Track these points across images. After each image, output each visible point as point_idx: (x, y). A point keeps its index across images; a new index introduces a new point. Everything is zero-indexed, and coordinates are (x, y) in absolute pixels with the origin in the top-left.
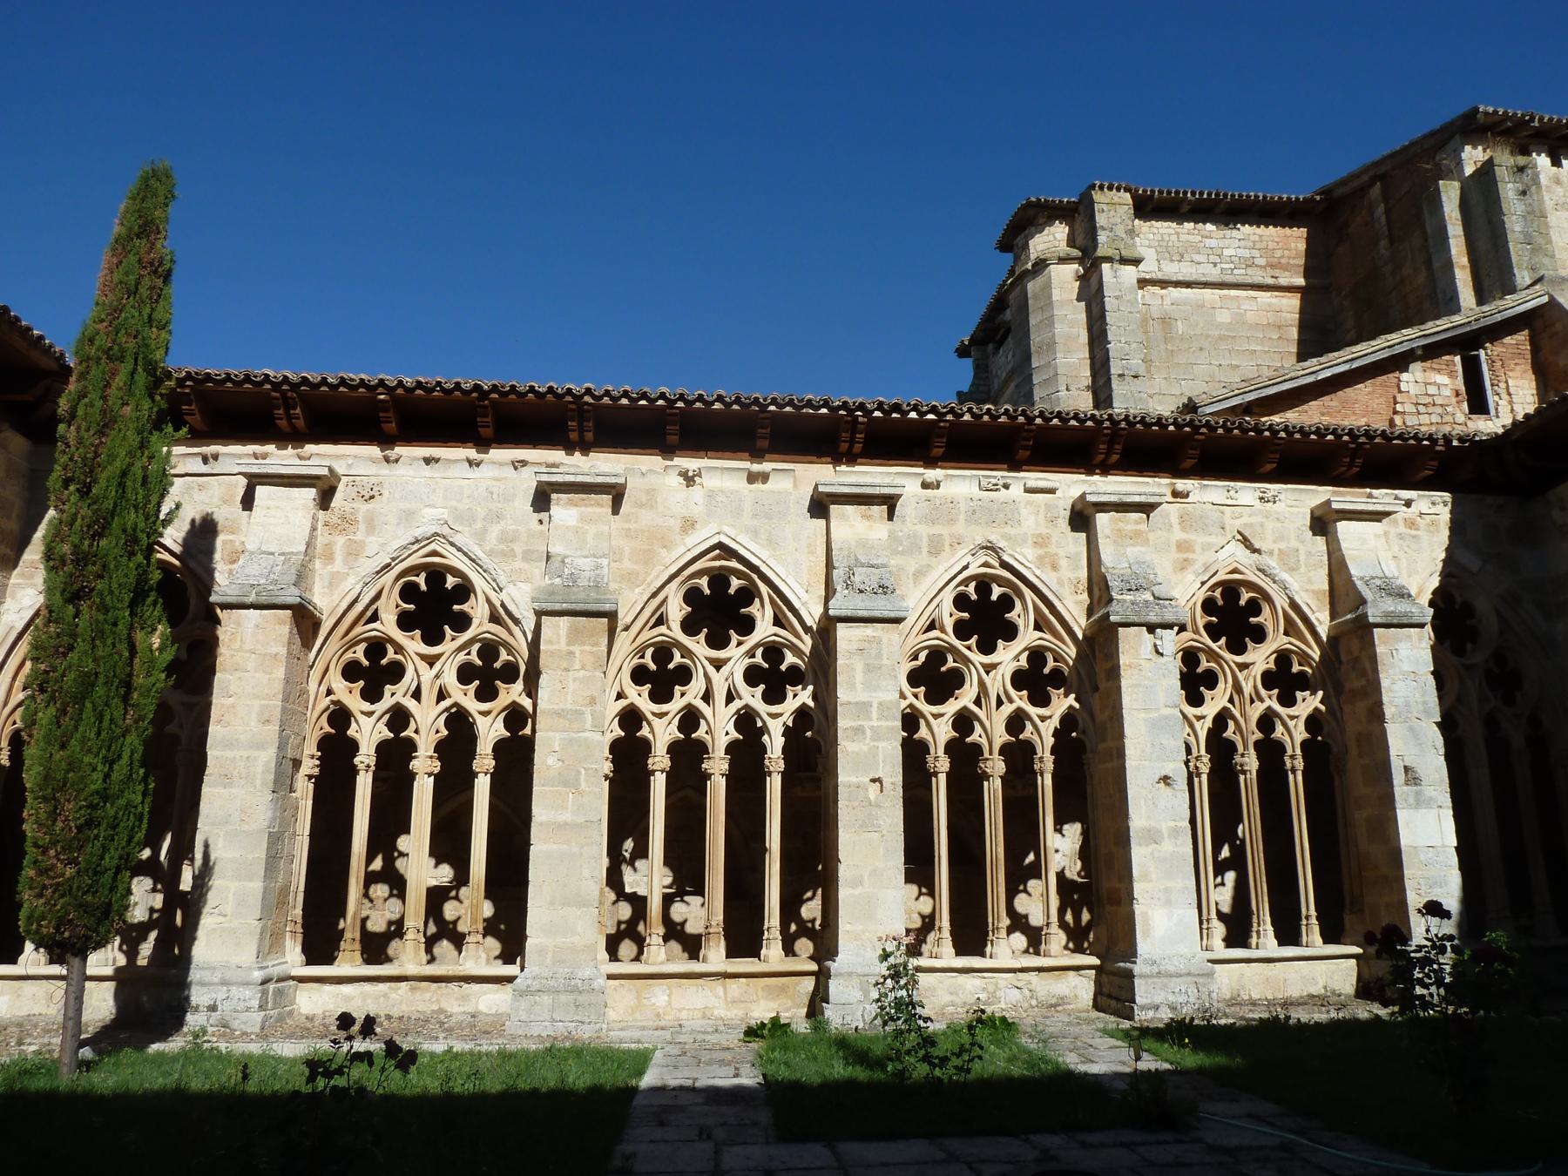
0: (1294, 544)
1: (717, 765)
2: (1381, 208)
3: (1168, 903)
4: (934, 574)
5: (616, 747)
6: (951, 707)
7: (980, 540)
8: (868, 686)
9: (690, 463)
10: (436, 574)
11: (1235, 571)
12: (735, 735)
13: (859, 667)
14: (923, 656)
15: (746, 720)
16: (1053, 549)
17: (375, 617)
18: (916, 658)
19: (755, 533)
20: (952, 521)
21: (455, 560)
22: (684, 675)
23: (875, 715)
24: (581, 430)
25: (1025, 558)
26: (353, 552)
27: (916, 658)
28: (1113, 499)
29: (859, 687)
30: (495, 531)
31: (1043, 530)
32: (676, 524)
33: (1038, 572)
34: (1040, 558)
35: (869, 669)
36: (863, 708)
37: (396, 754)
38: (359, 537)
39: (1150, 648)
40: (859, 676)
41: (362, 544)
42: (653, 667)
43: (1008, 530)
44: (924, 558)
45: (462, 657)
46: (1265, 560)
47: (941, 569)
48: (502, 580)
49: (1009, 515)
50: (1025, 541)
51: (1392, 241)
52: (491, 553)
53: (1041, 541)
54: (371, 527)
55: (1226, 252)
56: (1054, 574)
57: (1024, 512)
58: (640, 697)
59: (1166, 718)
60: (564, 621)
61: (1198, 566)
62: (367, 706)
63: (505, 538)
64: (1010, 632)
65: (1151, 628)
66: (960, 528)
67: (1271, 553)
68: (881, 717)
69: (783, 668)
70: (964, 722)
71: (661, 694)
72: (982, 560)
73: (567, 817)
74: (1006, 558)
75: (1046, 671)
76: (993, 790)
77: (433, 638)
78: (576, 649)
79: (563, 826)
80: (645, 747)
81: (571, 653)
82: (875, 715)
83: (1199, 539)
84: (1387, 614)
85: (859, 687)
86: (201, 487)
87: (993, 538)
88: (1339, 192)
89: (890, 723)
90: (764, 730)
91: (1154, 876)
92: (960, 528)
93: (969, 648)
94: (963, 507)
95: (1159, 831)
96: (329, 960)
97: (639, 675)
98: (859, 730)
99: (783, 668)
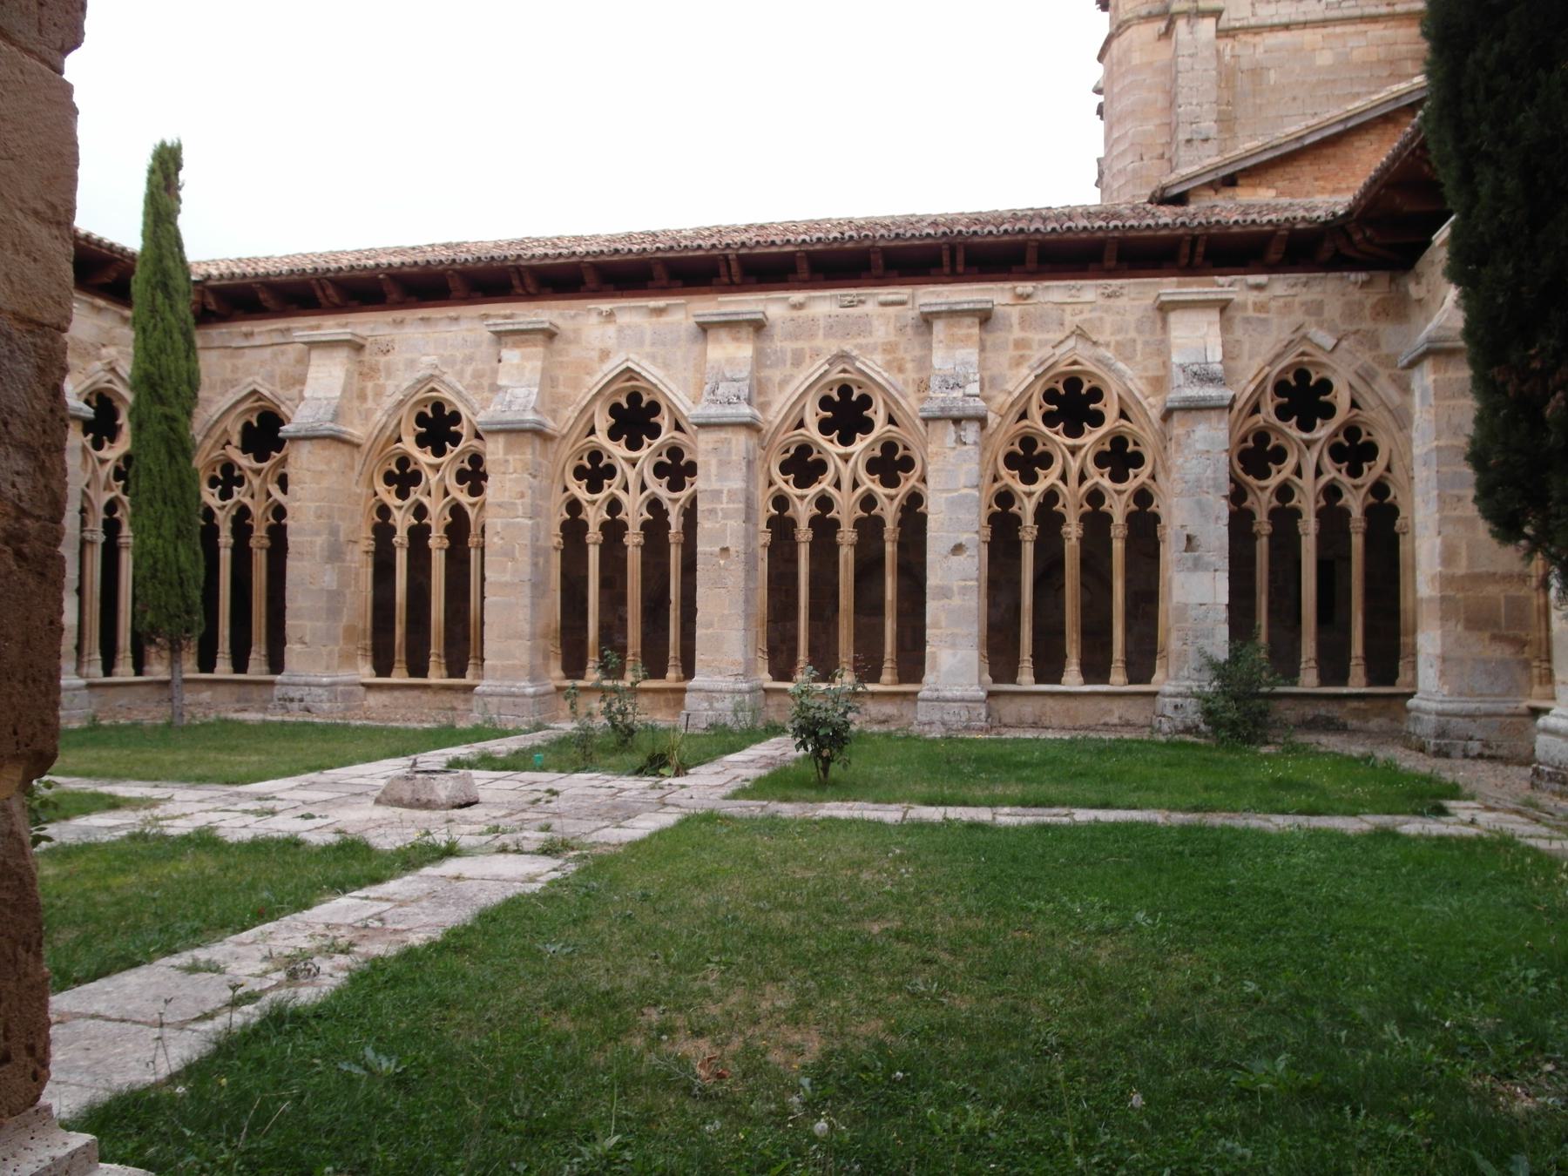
0: (1132, 334)
1: (633, 539)
3: (953, 646)
4: (796, 383)
5: (565, 526)
7: (834, 351)
8: (721, 477)
9: (605, 305)
10: (438, 406)
11: (1075, 363)
12: (647, 516)
13: (714, 462)
14: (792, 451)
15: (655, 505)
16: (901, 354)
17: (399, 440)
18: (787, 451)
19: (653, 358)
20: (812, 336)
21: (445, 394)
22: (610, 471)
23: (725, 499)
24: (523, 285)
25: (874, 366)
26: (379, 394)
27: (787, 451)
28: (944, 308)
29: (713, 478)
30: (469, 370)
31: (893, 338)
32: (595, 355)
35: (721, 464)
36: (716, 494)
37: (419, 534)
38: (382, 381)
39: (954, 436)
40: (714, 470)
41: (383, 387)
42: (588, 466)
43: (861, 340)
44: (788, 369)
45: (458, 466)
46: (1102, 351)
47: (802, 377)
48: (477, 406)
50: (875, 349)
52: (467, 387)
53: (889, 348)
54: (389, 375)
56: (901, 377)
57: (876, 323)
58: (579, 491)
59: (966, 496)
60: (501, 439)
61: (1034, 361)
62: (399, 502)
63: (478, 375)
64: (867, 426)
65: (957, 421)
66: (819, 342)
67: (1107, 345)
68: (730, 501)
69: (682, 463)
70: (824, 502)
71: (594, 487)
73: (507, 578)
74: (858, 364)
76: (846, 555)
77: (439, 451)
78: (510, 458)
79: (506, 584)
80: (584, 526)
81: (507, 461)
82: (725, 499)
83: (1035, 336)
84: (1187, 399)
85: (713, 478)
86: (283, 353)
87: (847, 348)
90: (666, 513)
92: (819, 342)
94: (822, 323)
95: (950, 589)
96: (388, 675)
97: (579, 473)
98: (712, 511)
99: (682, 463)
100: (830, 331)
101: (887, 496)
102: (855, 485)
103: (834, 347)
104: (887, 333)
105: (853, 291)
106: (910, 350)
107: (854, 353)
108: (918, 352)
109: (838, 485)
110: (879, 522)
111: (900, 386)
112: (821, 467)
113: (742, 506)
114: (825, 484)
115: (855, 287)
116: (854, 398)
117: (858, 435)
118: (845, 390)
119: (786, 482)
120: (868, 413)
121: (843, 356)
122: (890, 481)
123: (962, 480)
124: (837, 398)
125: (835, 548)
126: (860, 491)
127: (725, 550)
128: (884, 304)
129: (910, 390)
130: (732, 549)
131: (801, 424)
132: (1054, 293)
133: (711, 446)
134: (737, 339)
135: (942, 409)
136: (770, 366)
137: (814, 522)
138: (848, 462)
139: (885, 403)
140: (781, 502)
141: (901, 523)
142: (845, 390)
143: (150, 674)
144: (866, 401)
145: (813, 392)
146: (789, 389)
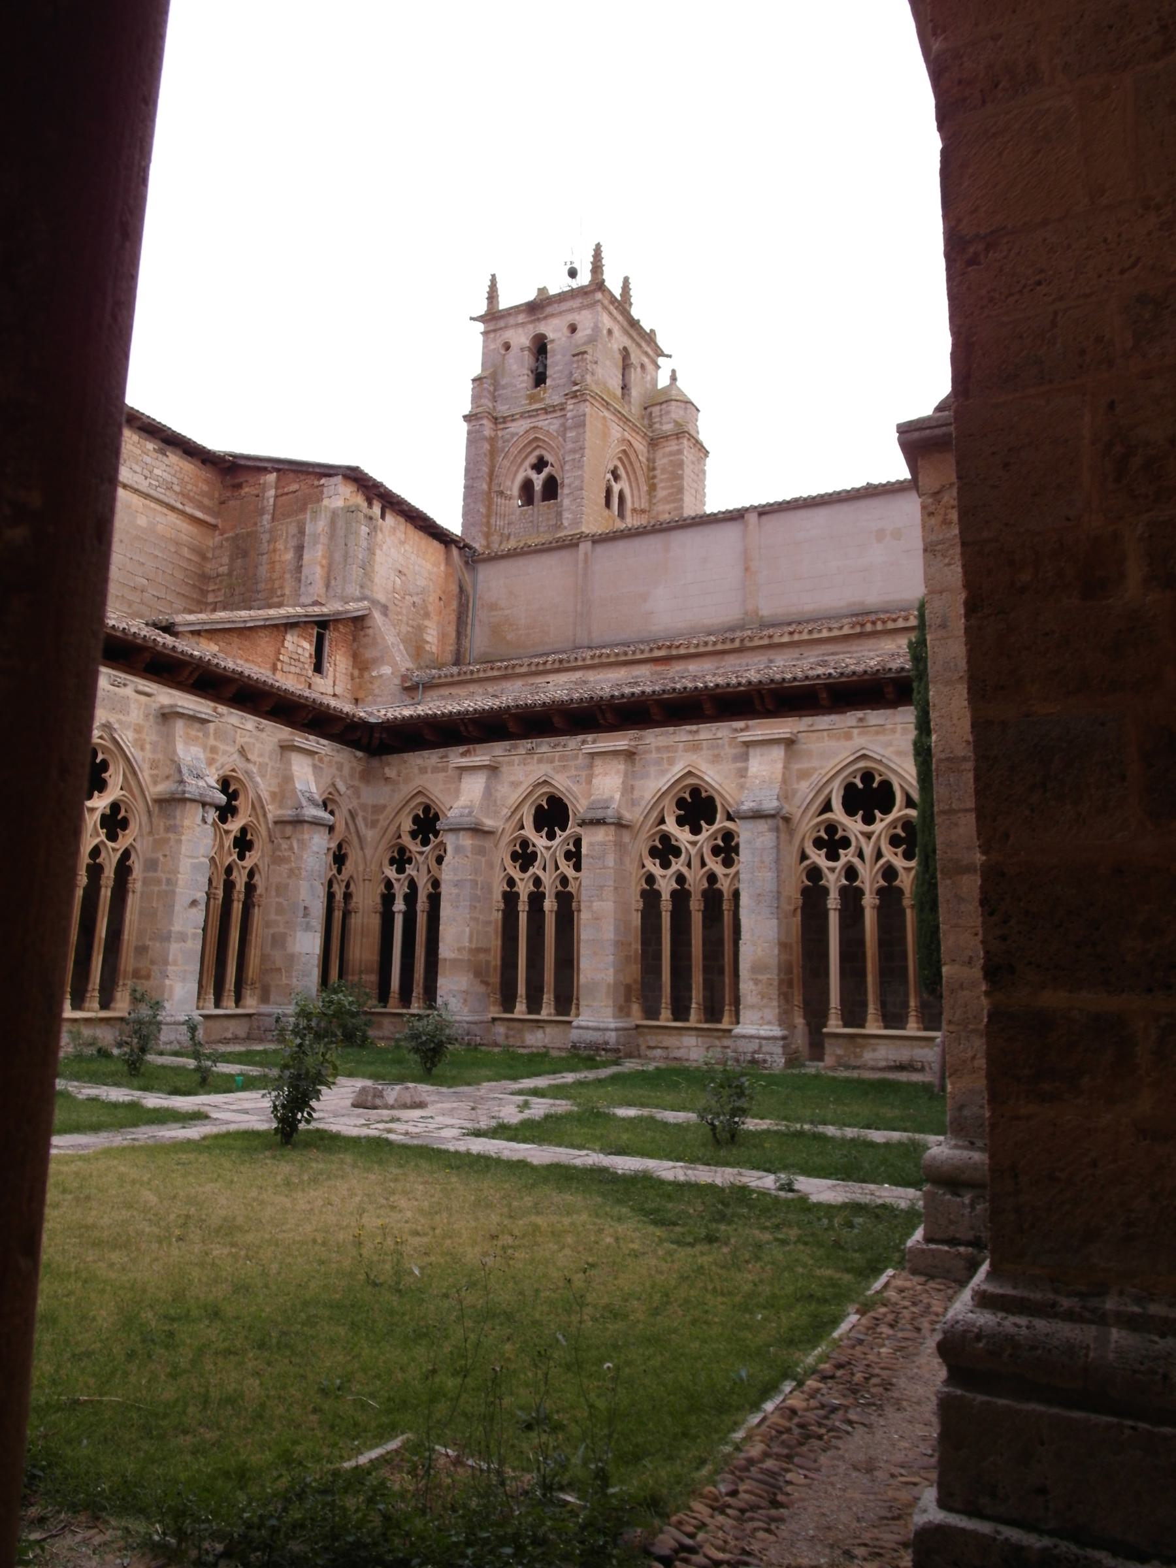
0: (267, 760)
2: (272, 492)
3: (184, 980)
11: (233, 770)
16: (144, 736)
31: (141, 722)
34: (136, 740)
46: (251, 767)
51: (273, 519)
53: (138, 729)
55: (157, 472)
57: (132, 706)
59: (202, 863)
61: (218, 764)
65: (204, 804)
67: (255, 763)
75: (119, 817)
83: (222, 747)
84: (314, 817)
87: (112, 720)
88: (243, 462)
105: (123, 675)
107: (116, 726)
108: (154, 738)
111: (139, 759)
115: (113, 668)
123: (202, 851)
129: (146, 766)
132: (233, 718)
135: (201, 795)
143: (114, 1009)
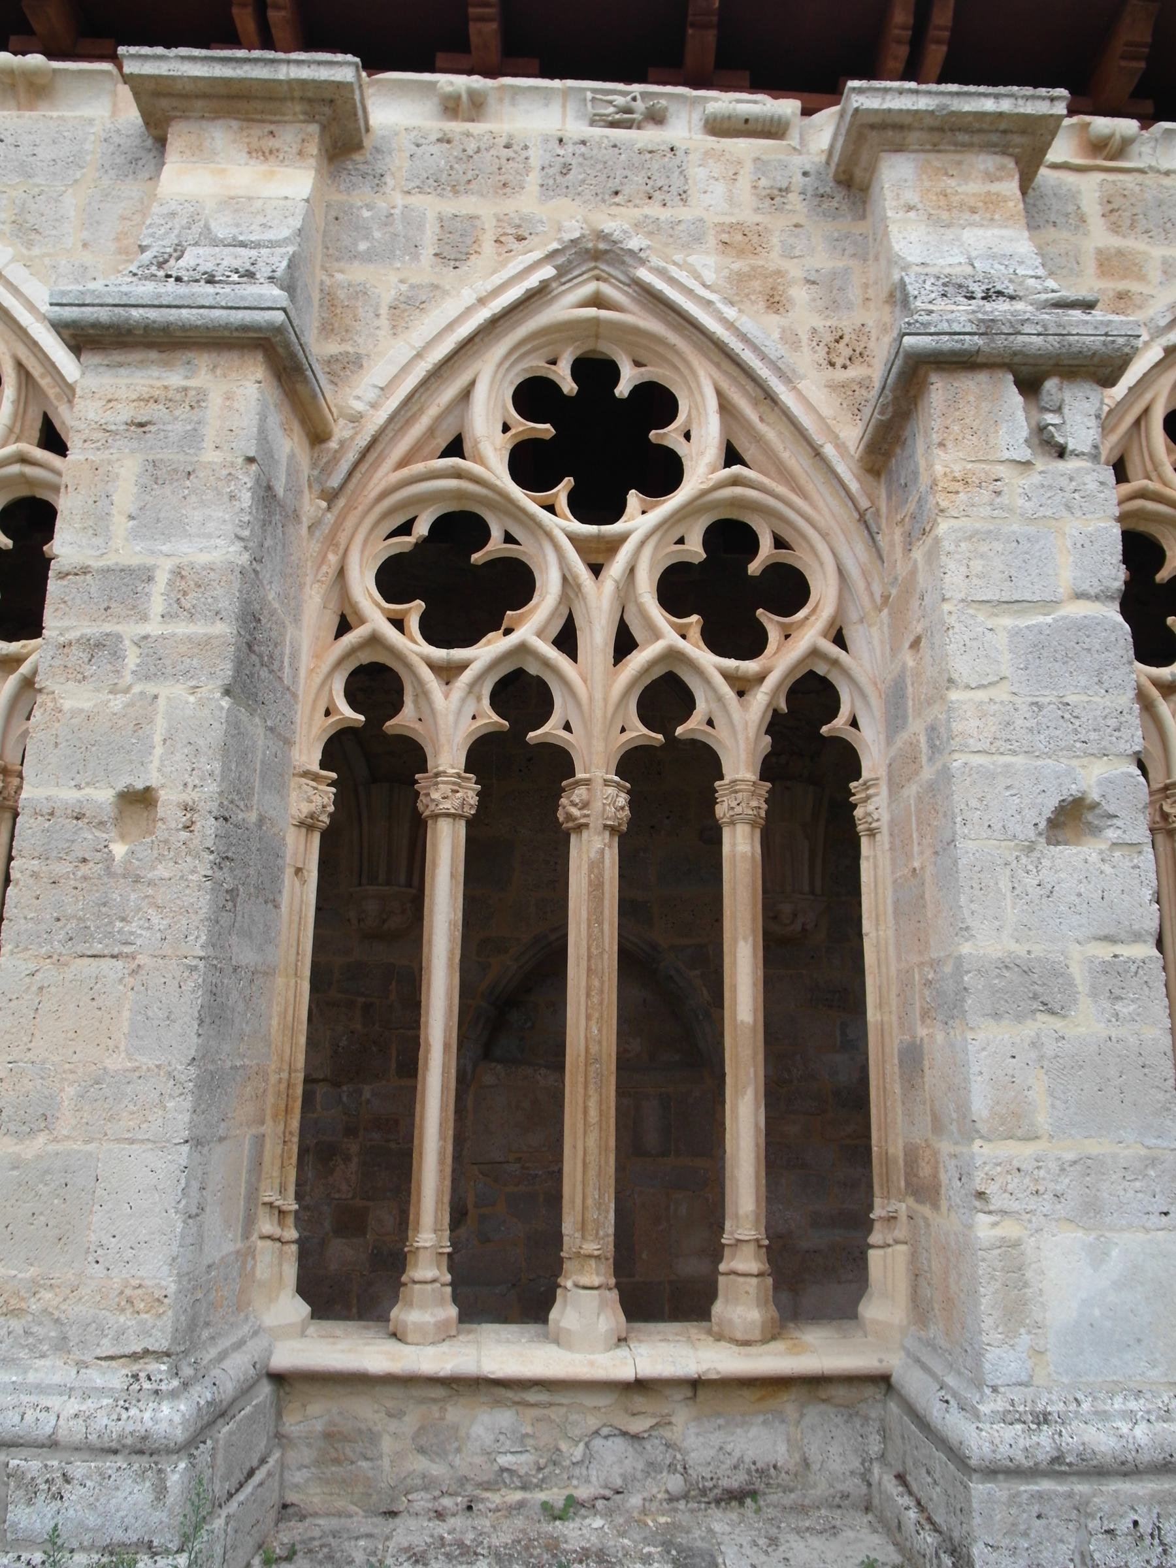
3: (1090, 1211)
4: (450, 308)
6: (489, 649)
7: (573, 230)
13: (128, 469)
14: (422, 529)
16: (774, 260)
18: (405, 529)
23: (157, 604)
25: (696, 277)
29: (120, 526)
31: (747, 214)
33: (730, 313)
34: (740, 280)
35: (156, 475)
40: (125, 493)
44: (424, 268)
47: (468, 296)
49: (664, 182)
50: (697, 239)
53: (738, 240)
56: (773, 320)
57: (698, 174)
59: (1082, 627)
64: (663, 474)
66: (526, 202)
68: (178, 609)
72: (587, 289)
74: (643, 274)
75: (755, 567)
76: (592, 866)
82: (157, 604)
85: (120, 526)
87: (609, 226)
89: (199, 629)
91: (1042, 1120)
92: (526, 202)
93: (551, 509)
95: (1058, 973)
98: (101, 648)
100: (560, 177)
101: (727, 676)
102: (624, 644)
103: (571, 219)
104: (731, 200)
106: (805, 250)
108: (823, 261)
109: (567, 640)
110: (704, 762)
111: (774, 347)
112: (514, 584)
113: (224, 629)
114: (531, 627)
116: (623, 389)
117: (634, 498)
118: (596, 371)
119: (398, 624)
120: (669, 436)
121: (595, 254)
122: (736, 637)
123: (1066, 576)
124: (569, 386)
125: (555, 843)
126: (638, 660)
127: (139, 801)
128: (719, 127)
129: (806, 361)
130: (169, 798)
131: (455, 448)
133: (126, 413)
134: (266, 154)
136: (367, 258)
137: (483, 756)
138: (596, 589)
139: (725, 407)
140: (375, 685)
141: (769, 769)
142: (596, 371)
144: (657, 403)
145: (499, 350)
146: (425, 327)
